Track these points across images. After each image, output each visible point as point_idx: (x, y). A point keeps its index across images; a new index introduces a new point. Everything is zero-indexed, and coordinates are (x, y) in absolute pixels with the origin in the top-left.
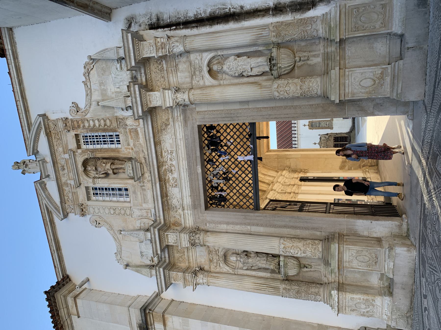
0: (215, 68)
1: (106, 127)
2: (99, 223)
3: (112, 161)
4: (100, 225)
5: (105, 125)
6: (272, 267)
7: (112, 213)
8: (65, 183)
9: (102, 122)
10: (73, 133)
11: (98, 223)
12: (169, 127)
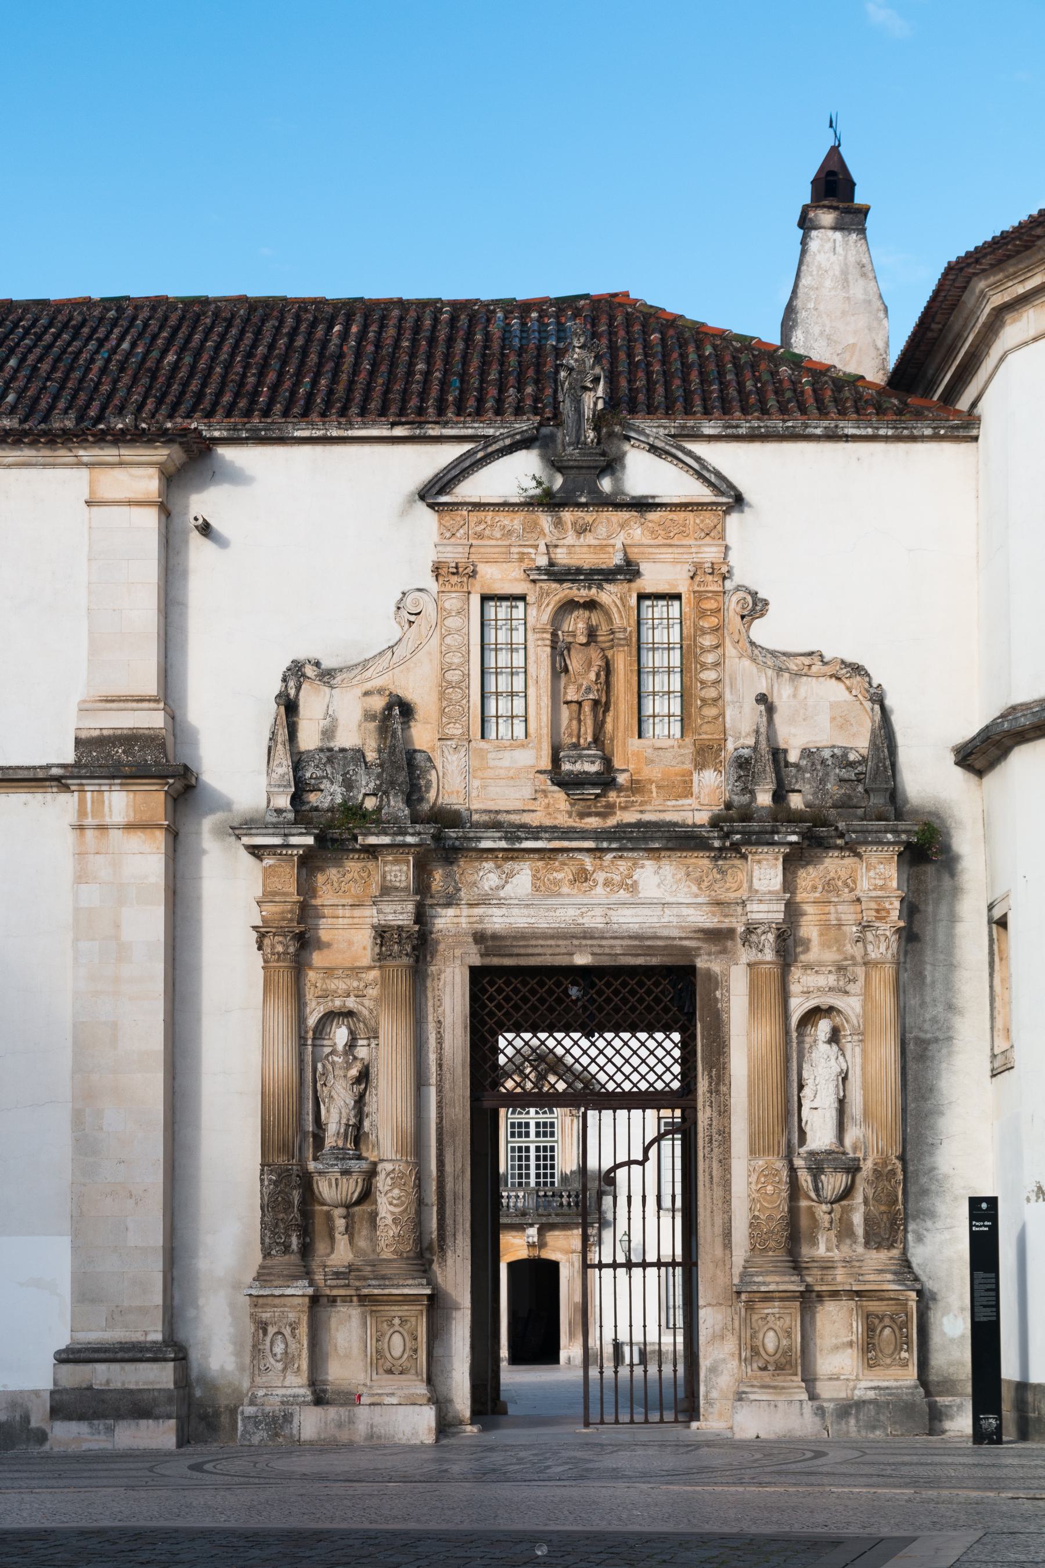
0: (824, 1027)
1: (699, 702)
2: (411, 623)
3: (604, 700)
4: (407, 626)
5: (703, 700)
6: (330, 1141)
7: (449, 676)
8: (536, 524)
9: (711, 693)
10: (683, 588)
11: (412, 618)
12: (694, 889)
